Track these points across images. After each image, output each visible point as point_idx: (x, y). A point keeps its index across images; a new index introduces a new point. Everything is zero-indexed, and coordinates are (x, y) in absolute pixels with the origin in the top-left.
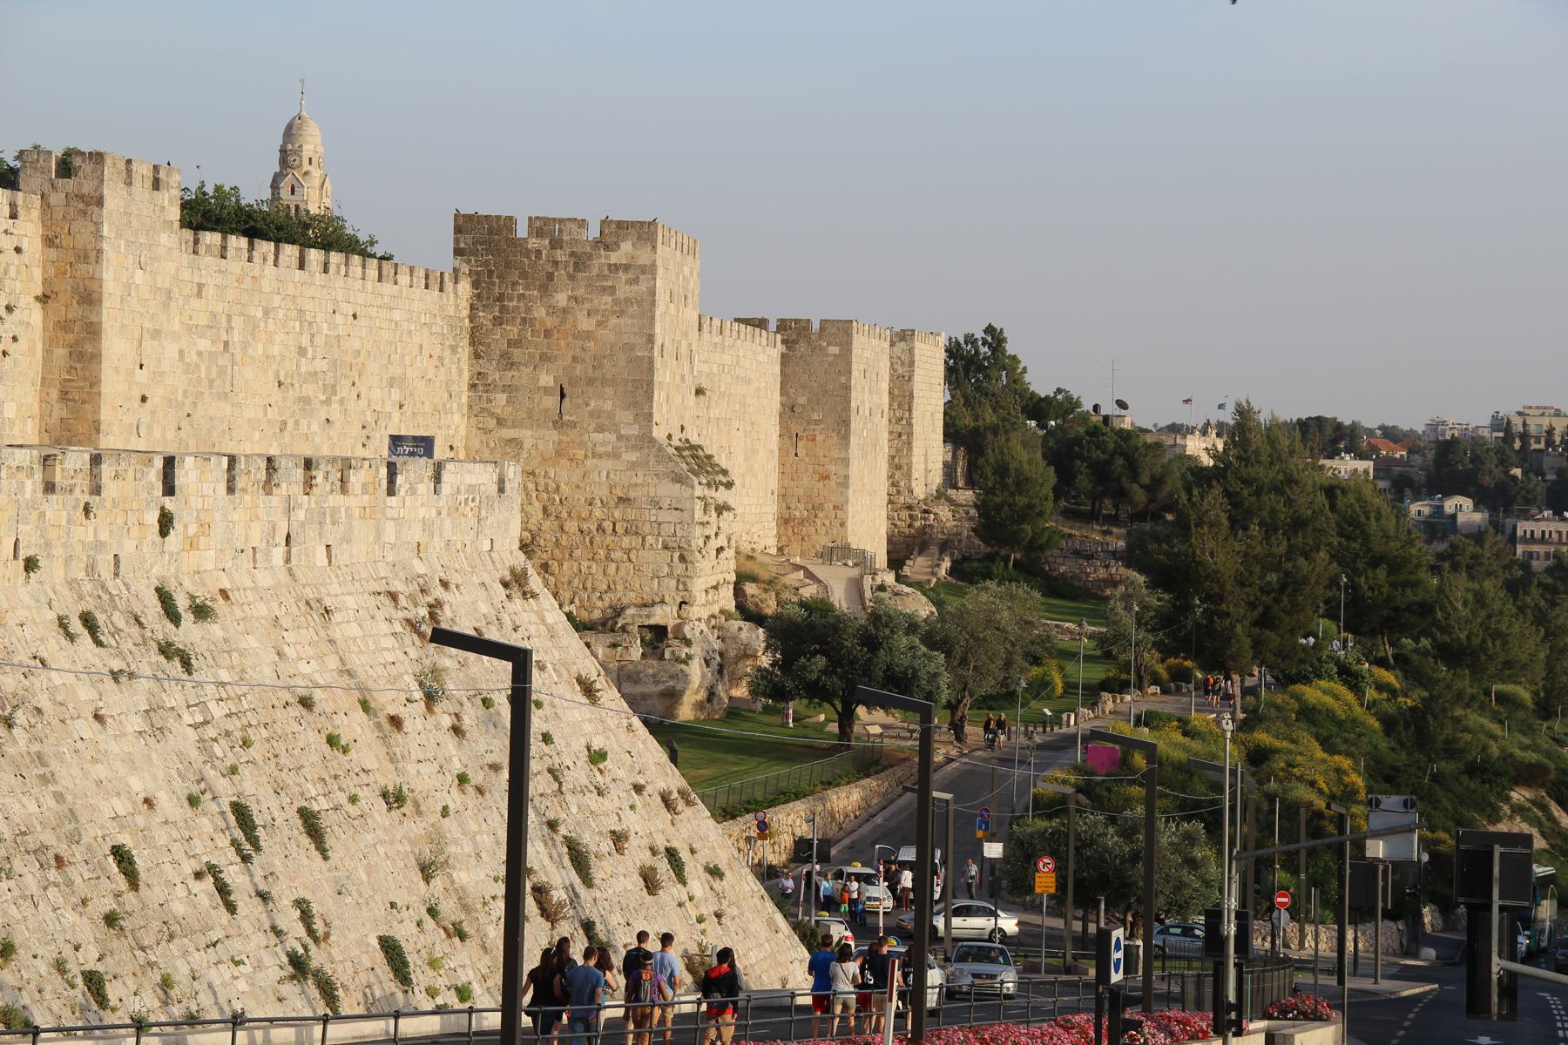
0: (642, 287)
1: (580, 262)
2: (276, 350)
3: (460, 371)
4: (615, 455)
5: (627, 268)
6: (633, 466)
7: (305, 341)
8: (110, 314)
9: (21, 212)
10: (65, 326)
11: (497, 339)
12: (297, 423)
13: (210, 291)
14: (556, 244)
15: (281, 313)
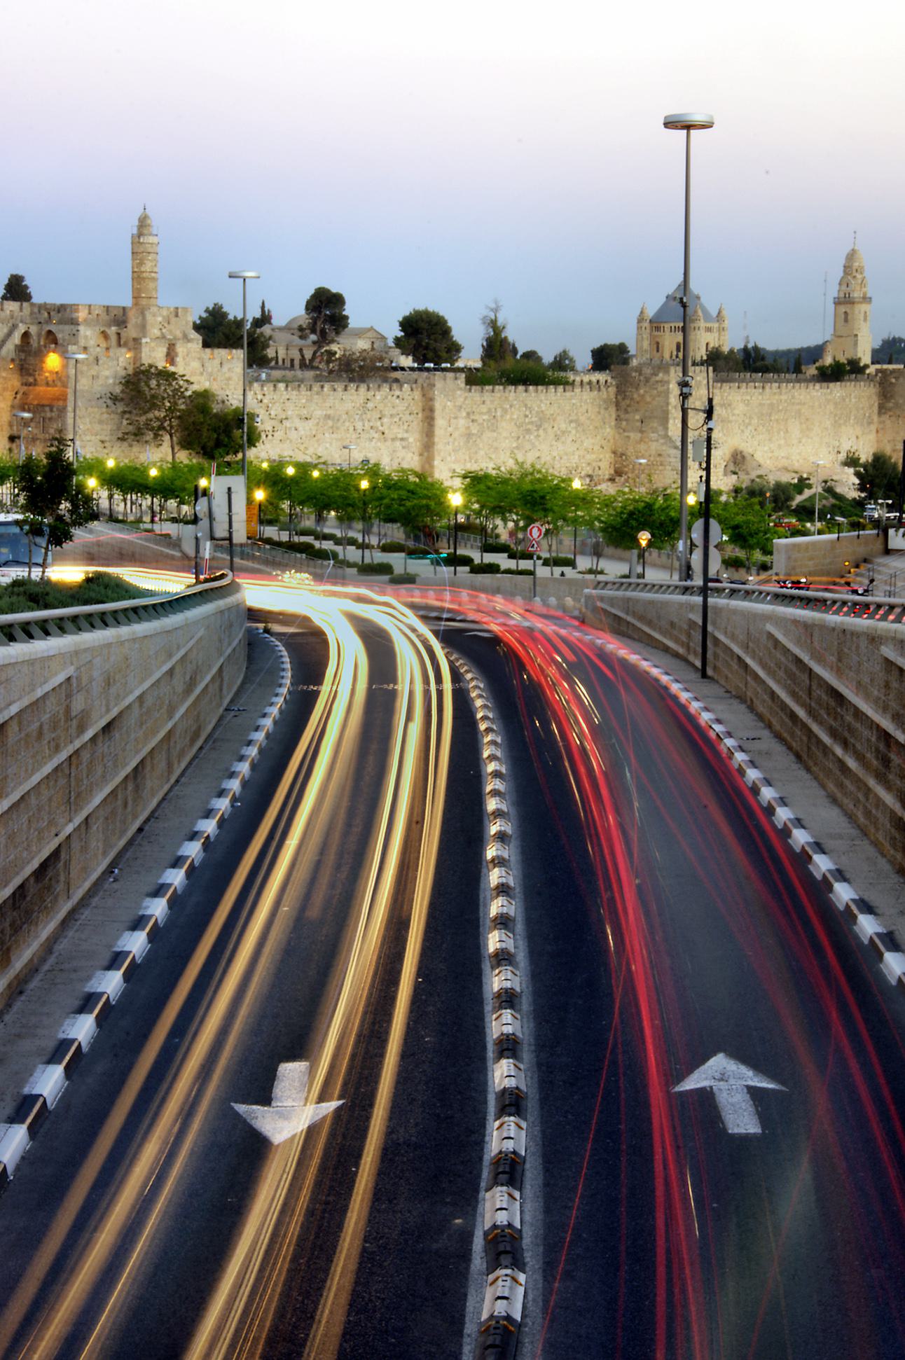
0: (665, 387)
1: (647, 380)
2: (515, 417)
3: (610, 415)
4: (657, 441)
5: (661, 381)
6: (662, 444)
7: (527, 413)
8: (438, 414)
9: (415, 389)
10: (427, 418)
11: (624, 404)
12: (524, 437)
13: (488, 402)
14: (640, 374)
15: (517, 406)
